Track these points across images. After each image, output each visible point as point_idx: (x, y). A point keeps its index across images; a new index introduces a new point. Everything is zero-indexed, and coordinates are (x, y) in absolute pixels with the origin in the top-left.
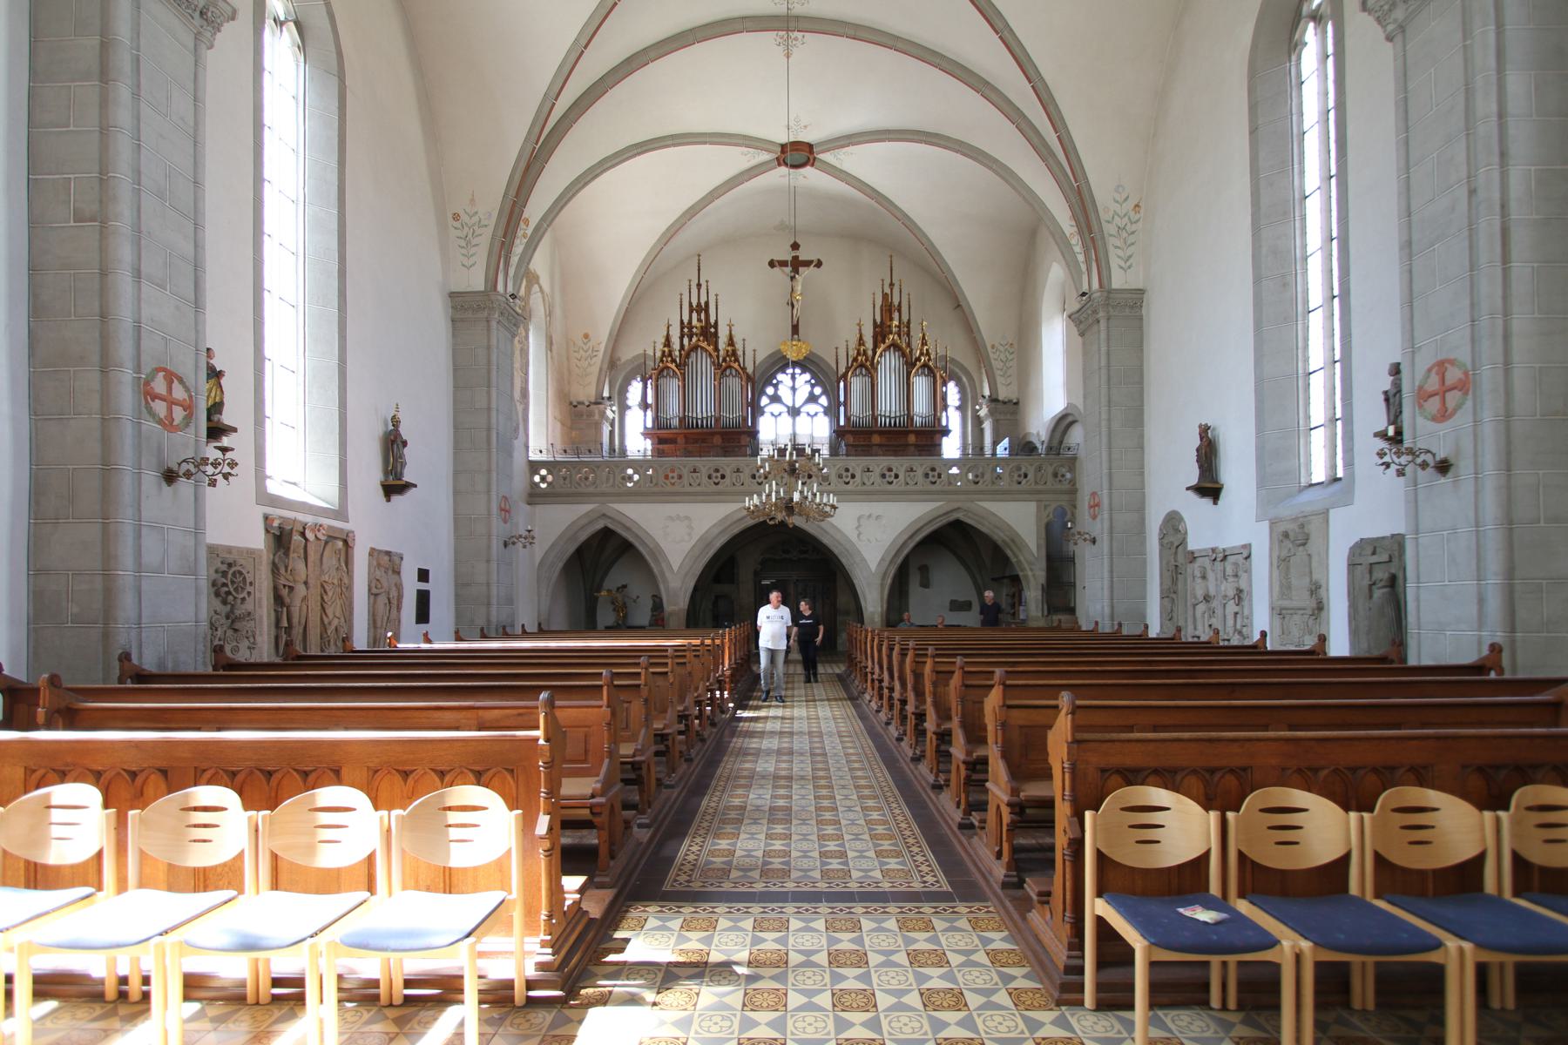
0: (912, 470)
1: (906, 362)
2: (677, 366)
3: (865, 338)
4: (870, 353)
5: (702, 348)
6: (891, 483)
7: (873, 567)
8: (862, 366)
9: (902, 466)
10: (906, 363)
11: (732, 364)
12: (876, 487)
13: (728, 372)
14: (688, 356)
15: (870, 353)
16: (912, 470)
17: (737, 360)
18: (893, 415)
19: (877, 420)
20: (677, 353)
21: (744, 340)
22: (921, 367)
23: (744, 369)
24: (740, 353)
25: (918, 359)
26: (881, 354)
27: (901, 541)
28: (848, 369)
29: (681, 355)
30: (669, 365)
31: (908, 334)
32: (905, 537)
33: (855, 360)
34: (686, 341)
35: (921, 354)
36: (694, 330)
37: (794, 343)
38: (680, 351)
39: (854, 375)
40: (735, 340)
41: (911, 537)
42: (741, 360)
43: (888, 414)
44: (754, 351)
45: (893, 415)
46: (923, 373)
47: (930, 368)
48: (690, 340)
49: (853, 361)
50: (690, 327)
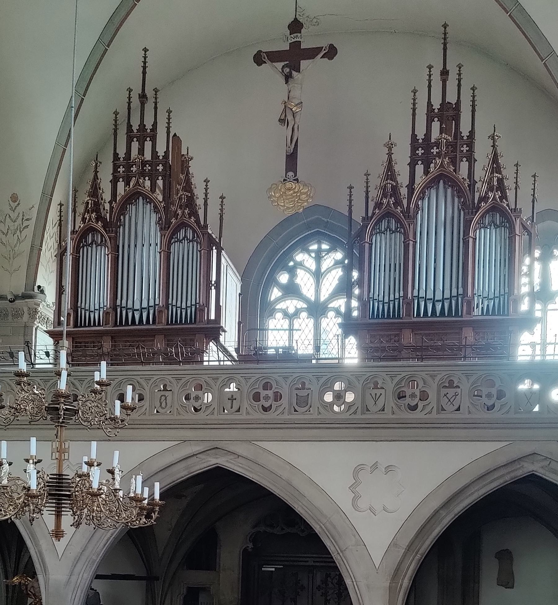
0: (451, 385)
1: (464, 204)
2: (104, 227)
3: (397, 168)
4: (404, 191)
5: (145, 197)
6: (414, 408)
7: (377, 556)
8: (388, 215)
9: (433, 377)
10: (464, 206)
11: (186, 220)
12: (388, 415)
13: (181, 234)
14: (123, 210)
15: (404, 191)
16: (451, 385)
17: (194, 213)
18: (439, 296)
19: (409, 304)
20: (107, 206)
21: (207, 181)
22: (487, 212)
23: (206, 226)
24: (200, 202)
25: (484, 199)
26: (423, 192)
27: (427, 512)
28: (367, 219)
29: (112, 208)
30: (94, 225)
31: (471, 160)
32: (435, 504)
33: (378, 205)
34: (121, 185)
35: (491, 188)
36: (134, 169)
37: (288, 185)
38: (110, 202)
39: (377, 230)
40: (193, 181)
41: (446, 505)
42: (201, 213)
43: (430, 295)
44: (222, 198)
45: (439, 296)
46: (493, 223)
47: (504, 213)
48: (127, 184)
49: (375, 209)
50: (128, 165)
